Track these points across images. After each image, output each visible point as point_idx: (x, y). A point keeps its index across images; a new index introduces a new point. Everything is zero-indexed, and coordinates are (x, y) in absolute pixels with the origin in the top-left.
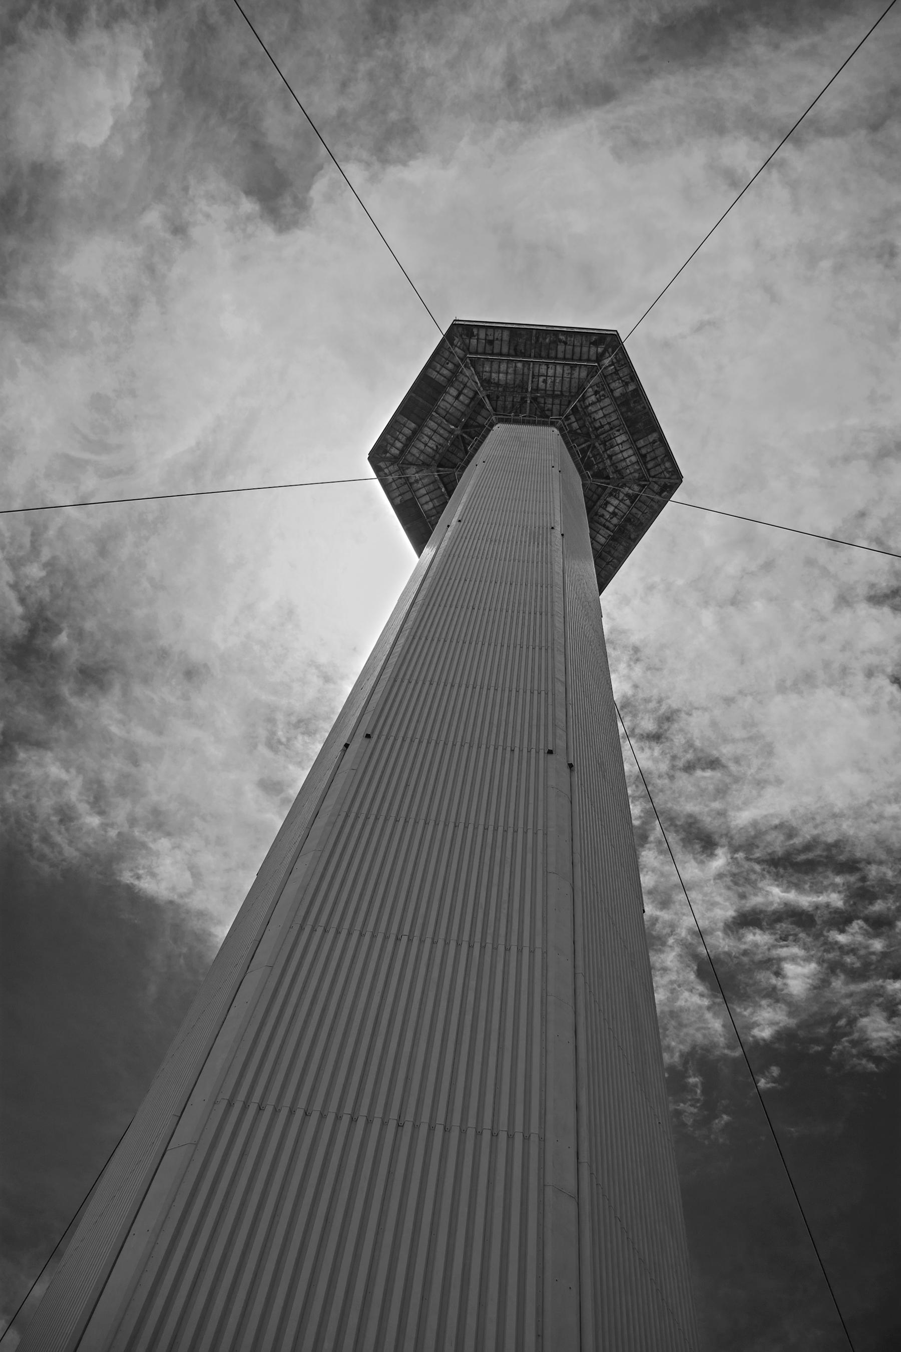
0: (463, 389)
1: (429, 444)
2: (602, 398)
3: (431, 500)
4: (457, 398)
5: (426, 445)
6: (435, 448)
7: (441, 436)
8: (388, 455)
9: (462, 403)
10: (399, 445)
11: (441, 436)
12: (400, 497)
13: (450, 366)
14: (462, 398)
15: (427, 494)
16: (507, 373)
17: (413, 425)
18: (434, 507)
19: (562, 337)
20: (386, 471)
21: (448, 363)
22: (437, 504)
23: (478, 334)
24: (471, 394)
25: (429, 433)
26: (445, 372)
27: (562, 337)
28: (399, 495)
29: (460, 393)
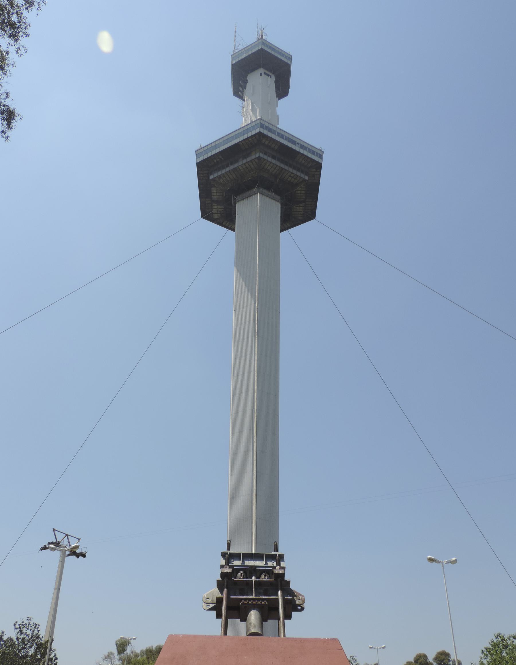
0: (294, 178)
1: (269, 167)
2: (291, 224)
3: (243, 169)
4: (290, 176)
5: (269, 166)
6: (268, 169)
7: (273, 171)
8: (262, 138)
9: (288, 178)
10: (267, 143)
11: (273, 171)
12: (241, 144)
13: (304, 161)
14: (290, 178)
15: (246, 167)
16: (301, 193)
17: (276, 148)
18: (240, 170)
19: (315, 200)
20: (254, 138)
21: (305, 160)
22: (242, 171)
23: (317, 171)
24: (292, 181)
25: (274, 167)
26: (301, 160)
27: (315, 200)
28: (242, 144)
29: (292, 177)
